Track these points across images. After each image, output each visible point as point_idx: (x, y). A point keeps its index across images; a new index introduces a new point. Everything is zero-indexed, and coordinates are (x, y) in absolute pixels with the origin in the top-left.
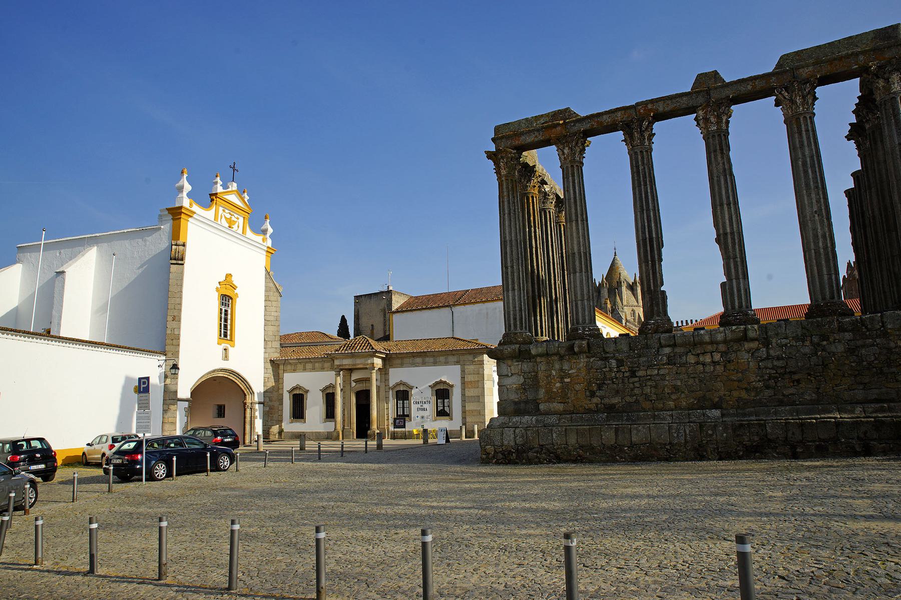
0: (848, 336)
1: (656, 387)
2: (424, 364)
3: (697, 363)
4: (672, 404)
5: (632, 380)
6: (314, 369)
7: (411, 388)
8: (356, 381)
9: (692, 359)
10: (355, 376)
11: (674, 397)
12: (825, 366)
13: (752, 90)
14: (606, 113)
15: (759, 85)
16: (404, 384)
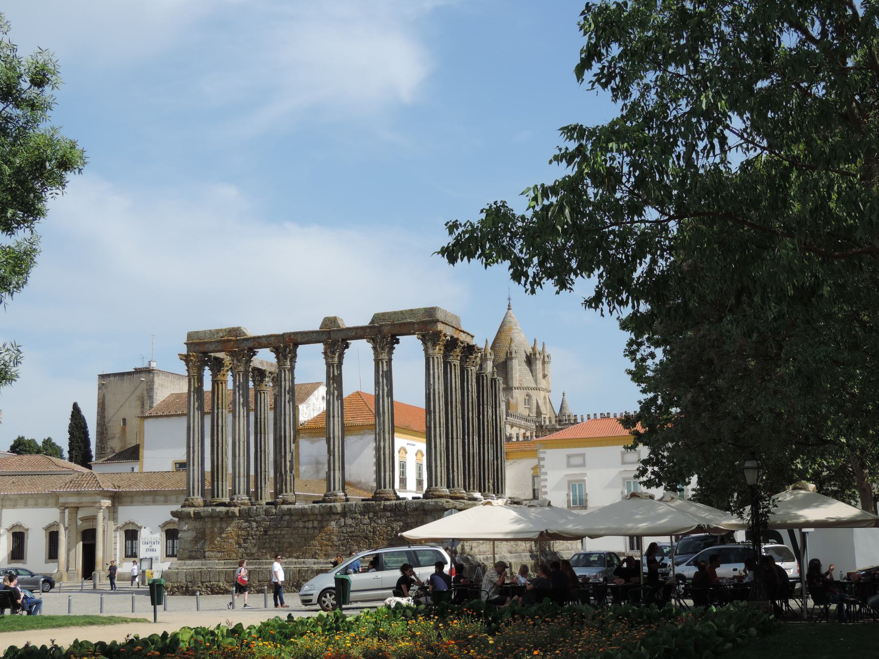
0: (388, 514)
1: (279, 543)
2: (154, 502)
3: (304, 527)
4: (287, 555)
5: (265, 537)
6: (36, 505)
7: (140, 528)
8: (82, 519)
9: (301, 525)
10: (81, 514)
11: (289, 550)
12: (374, 532)
13: (358, 333)
14: (264, 337)
15: (360, 332)
16: (133, 524)
